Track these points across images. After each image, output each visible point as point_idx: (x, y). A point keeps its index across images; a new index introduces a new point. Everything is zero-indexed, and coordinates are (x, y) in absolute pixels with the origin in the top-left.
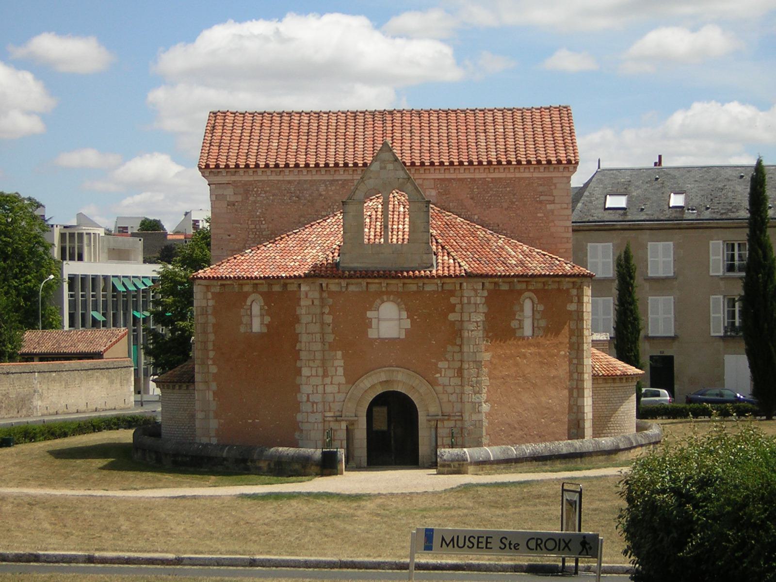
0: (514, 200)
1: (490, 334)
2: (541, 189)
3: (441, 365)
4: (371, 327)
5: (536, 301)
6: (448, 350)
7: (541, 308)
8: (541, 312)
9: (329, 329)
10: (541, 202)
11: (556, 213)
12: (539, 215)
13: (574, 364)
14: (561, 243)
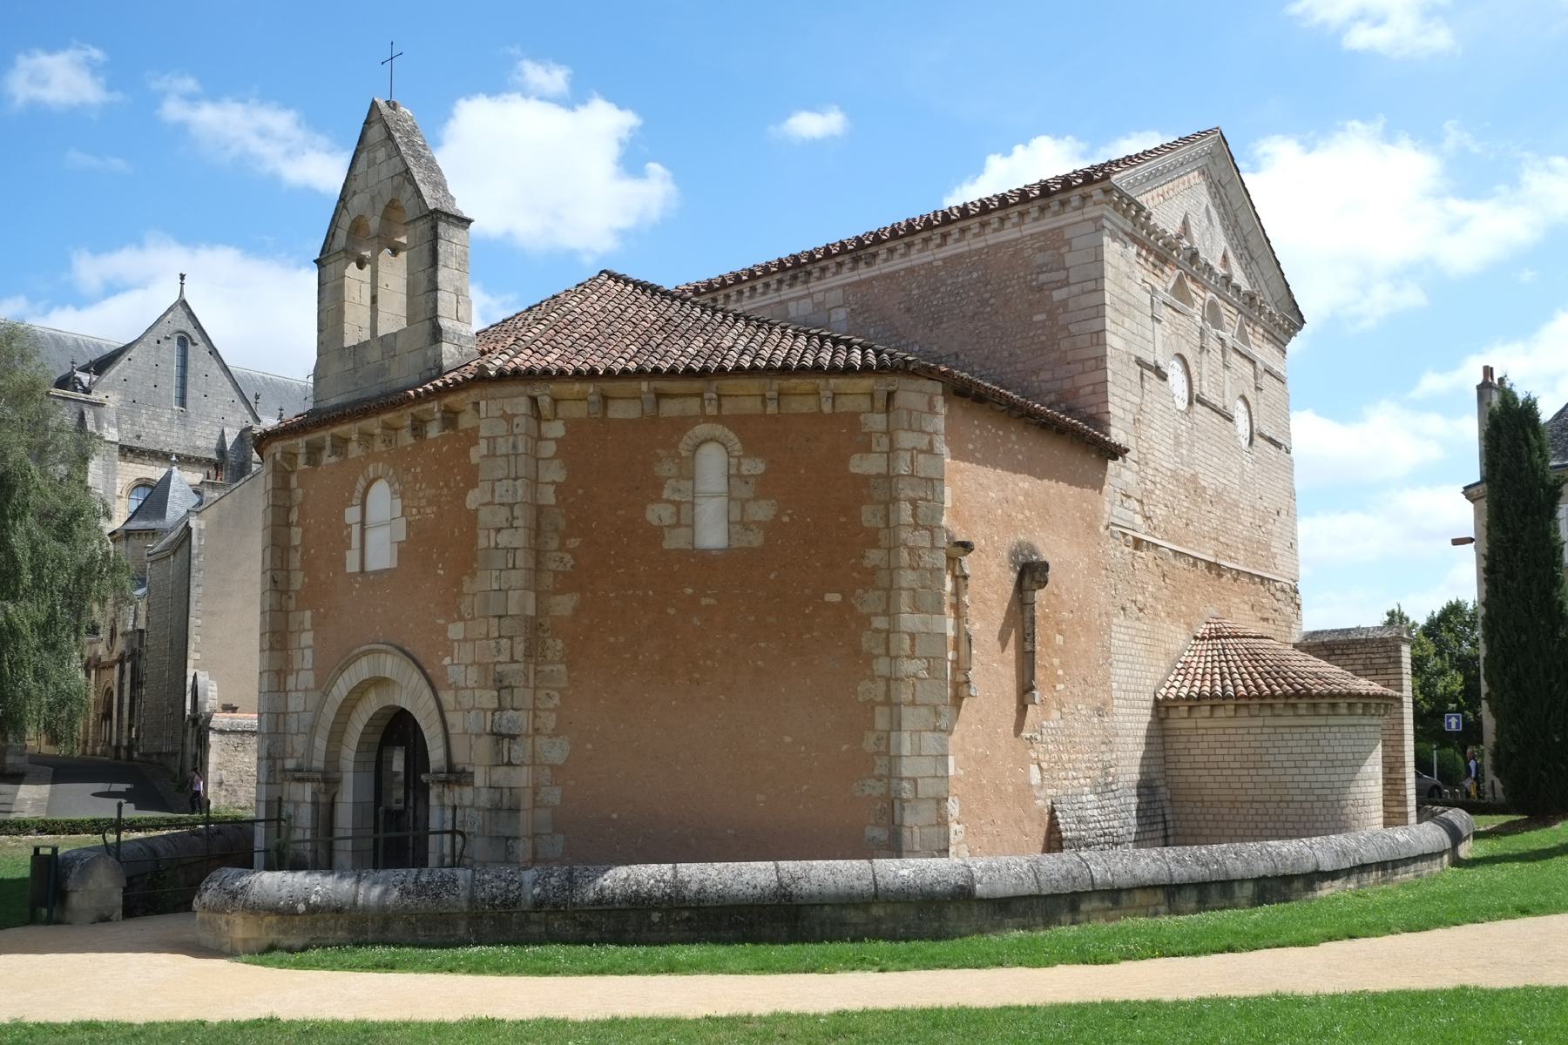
0: (987, 295)
1: (574, 543)
2: (1040, 258)
3: (455, 631)
5: (737, 447)
8: (752, 481)
10: (1040, 288)
12: (1037, 318)
14: (1083, 372)
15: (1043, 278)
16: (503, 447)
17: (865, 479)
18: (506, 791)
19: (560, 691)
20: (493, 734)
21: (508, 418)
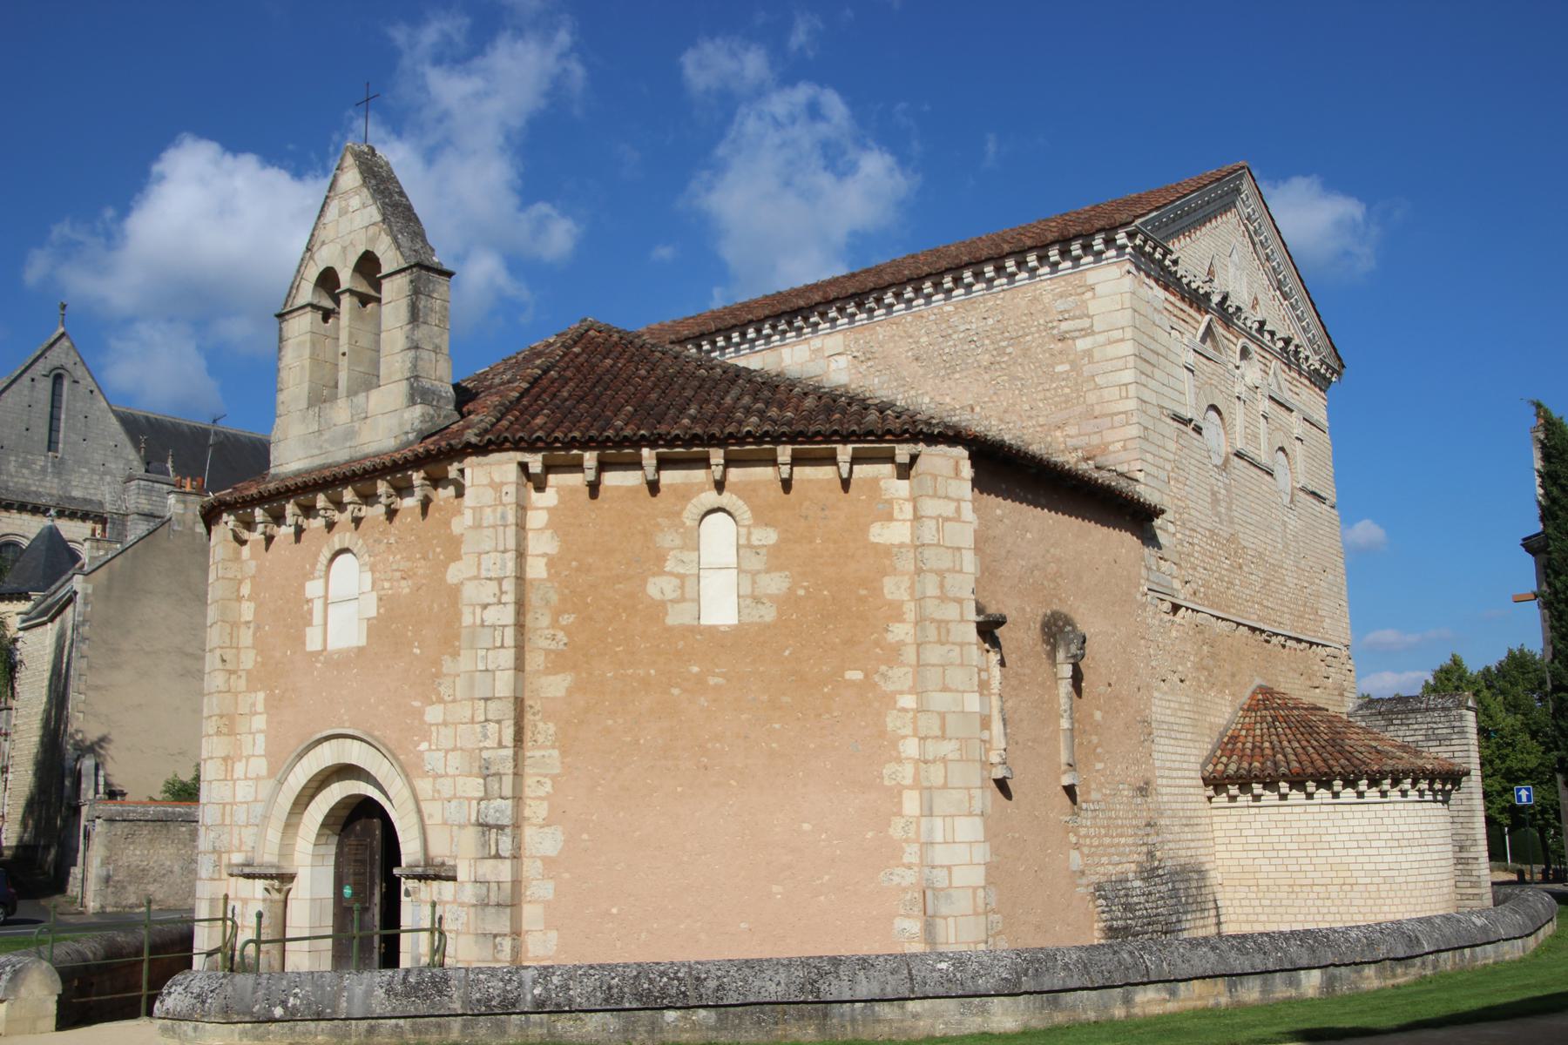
0: (1004, 344)
1: (566, 619)
2: (1060, 305)
3: (434, 714)
4: (310, 624)
6: (445, 670)
7: (767, 536)
8: (763, 551)
9: (246, 636)
11: (1097, 355)
12: (1059, 369)
13: (904, 710)
14: (1113, 428)
15: (1064, 326)
16: (489, 517)
17: (887, 551)
18: (494, 886)
19: (554, 778)
20: (481, 825)
21: (496, 487)
